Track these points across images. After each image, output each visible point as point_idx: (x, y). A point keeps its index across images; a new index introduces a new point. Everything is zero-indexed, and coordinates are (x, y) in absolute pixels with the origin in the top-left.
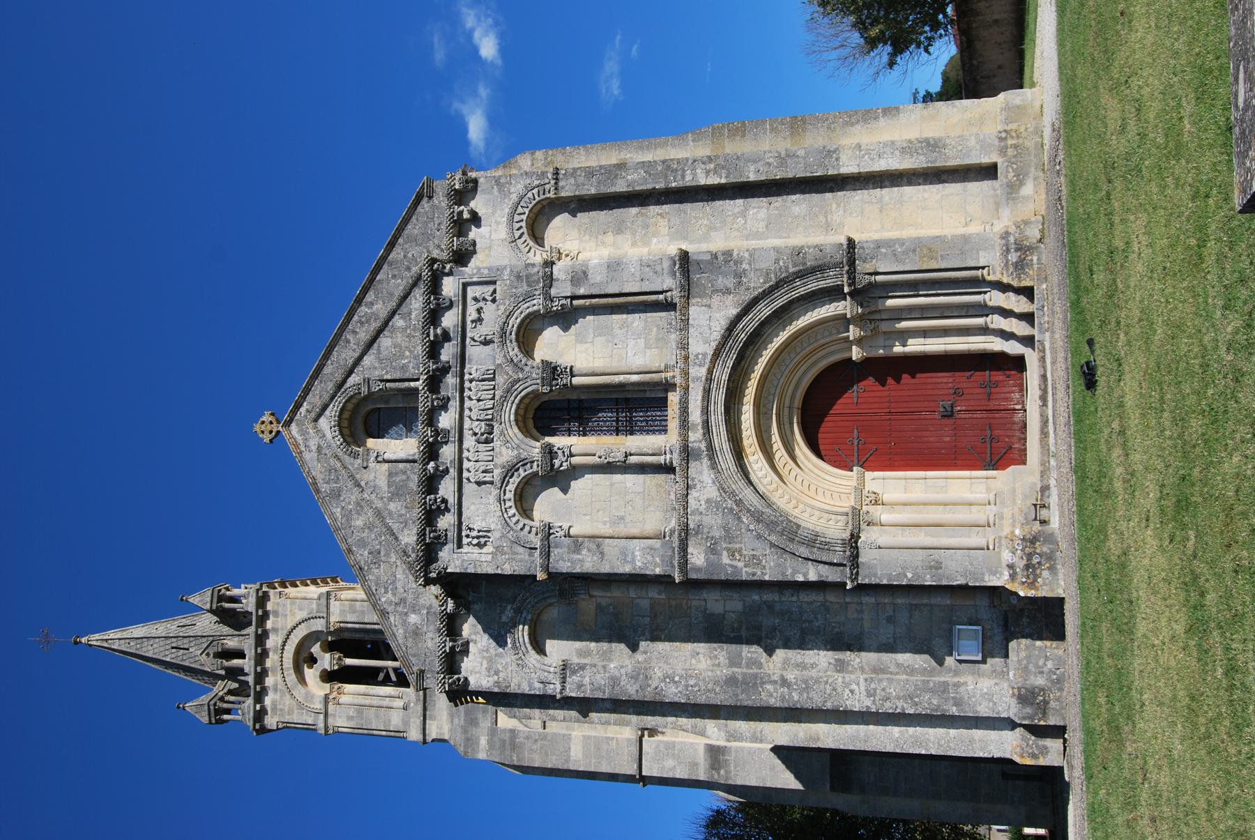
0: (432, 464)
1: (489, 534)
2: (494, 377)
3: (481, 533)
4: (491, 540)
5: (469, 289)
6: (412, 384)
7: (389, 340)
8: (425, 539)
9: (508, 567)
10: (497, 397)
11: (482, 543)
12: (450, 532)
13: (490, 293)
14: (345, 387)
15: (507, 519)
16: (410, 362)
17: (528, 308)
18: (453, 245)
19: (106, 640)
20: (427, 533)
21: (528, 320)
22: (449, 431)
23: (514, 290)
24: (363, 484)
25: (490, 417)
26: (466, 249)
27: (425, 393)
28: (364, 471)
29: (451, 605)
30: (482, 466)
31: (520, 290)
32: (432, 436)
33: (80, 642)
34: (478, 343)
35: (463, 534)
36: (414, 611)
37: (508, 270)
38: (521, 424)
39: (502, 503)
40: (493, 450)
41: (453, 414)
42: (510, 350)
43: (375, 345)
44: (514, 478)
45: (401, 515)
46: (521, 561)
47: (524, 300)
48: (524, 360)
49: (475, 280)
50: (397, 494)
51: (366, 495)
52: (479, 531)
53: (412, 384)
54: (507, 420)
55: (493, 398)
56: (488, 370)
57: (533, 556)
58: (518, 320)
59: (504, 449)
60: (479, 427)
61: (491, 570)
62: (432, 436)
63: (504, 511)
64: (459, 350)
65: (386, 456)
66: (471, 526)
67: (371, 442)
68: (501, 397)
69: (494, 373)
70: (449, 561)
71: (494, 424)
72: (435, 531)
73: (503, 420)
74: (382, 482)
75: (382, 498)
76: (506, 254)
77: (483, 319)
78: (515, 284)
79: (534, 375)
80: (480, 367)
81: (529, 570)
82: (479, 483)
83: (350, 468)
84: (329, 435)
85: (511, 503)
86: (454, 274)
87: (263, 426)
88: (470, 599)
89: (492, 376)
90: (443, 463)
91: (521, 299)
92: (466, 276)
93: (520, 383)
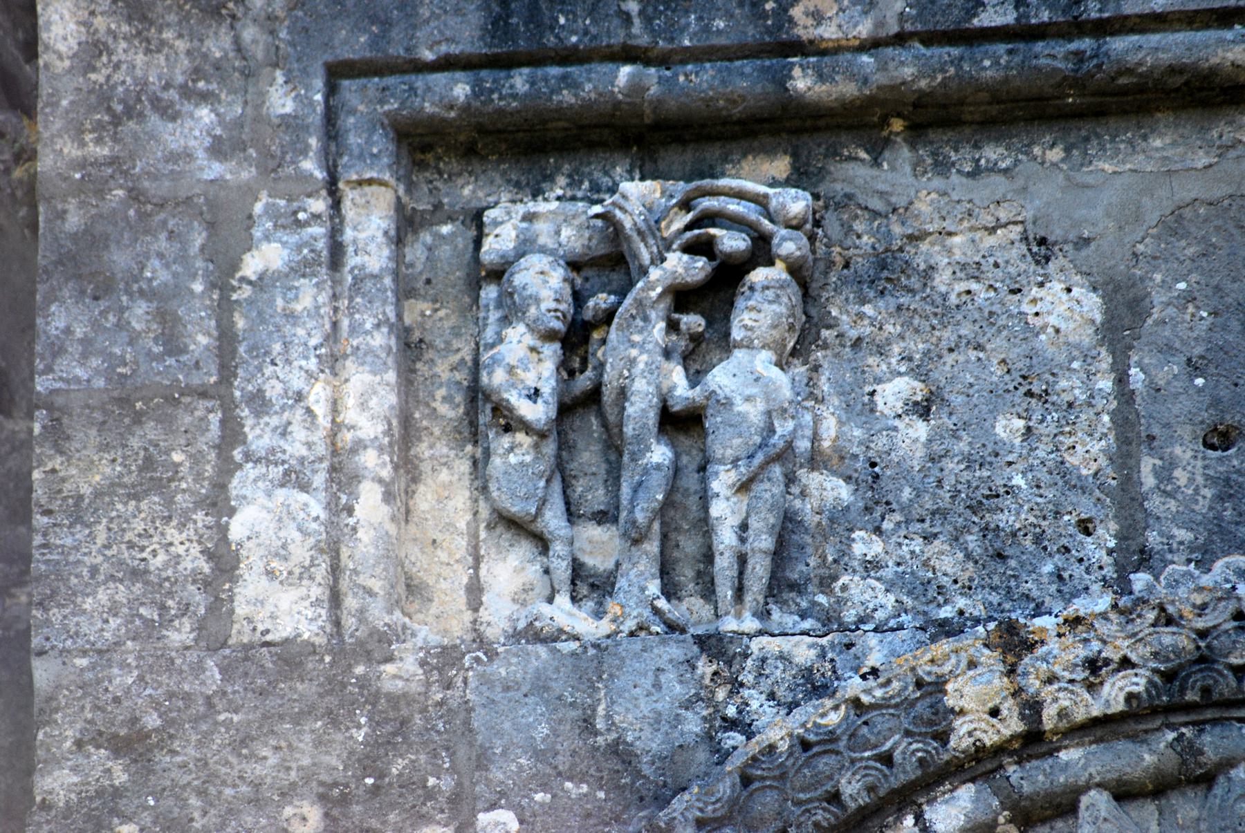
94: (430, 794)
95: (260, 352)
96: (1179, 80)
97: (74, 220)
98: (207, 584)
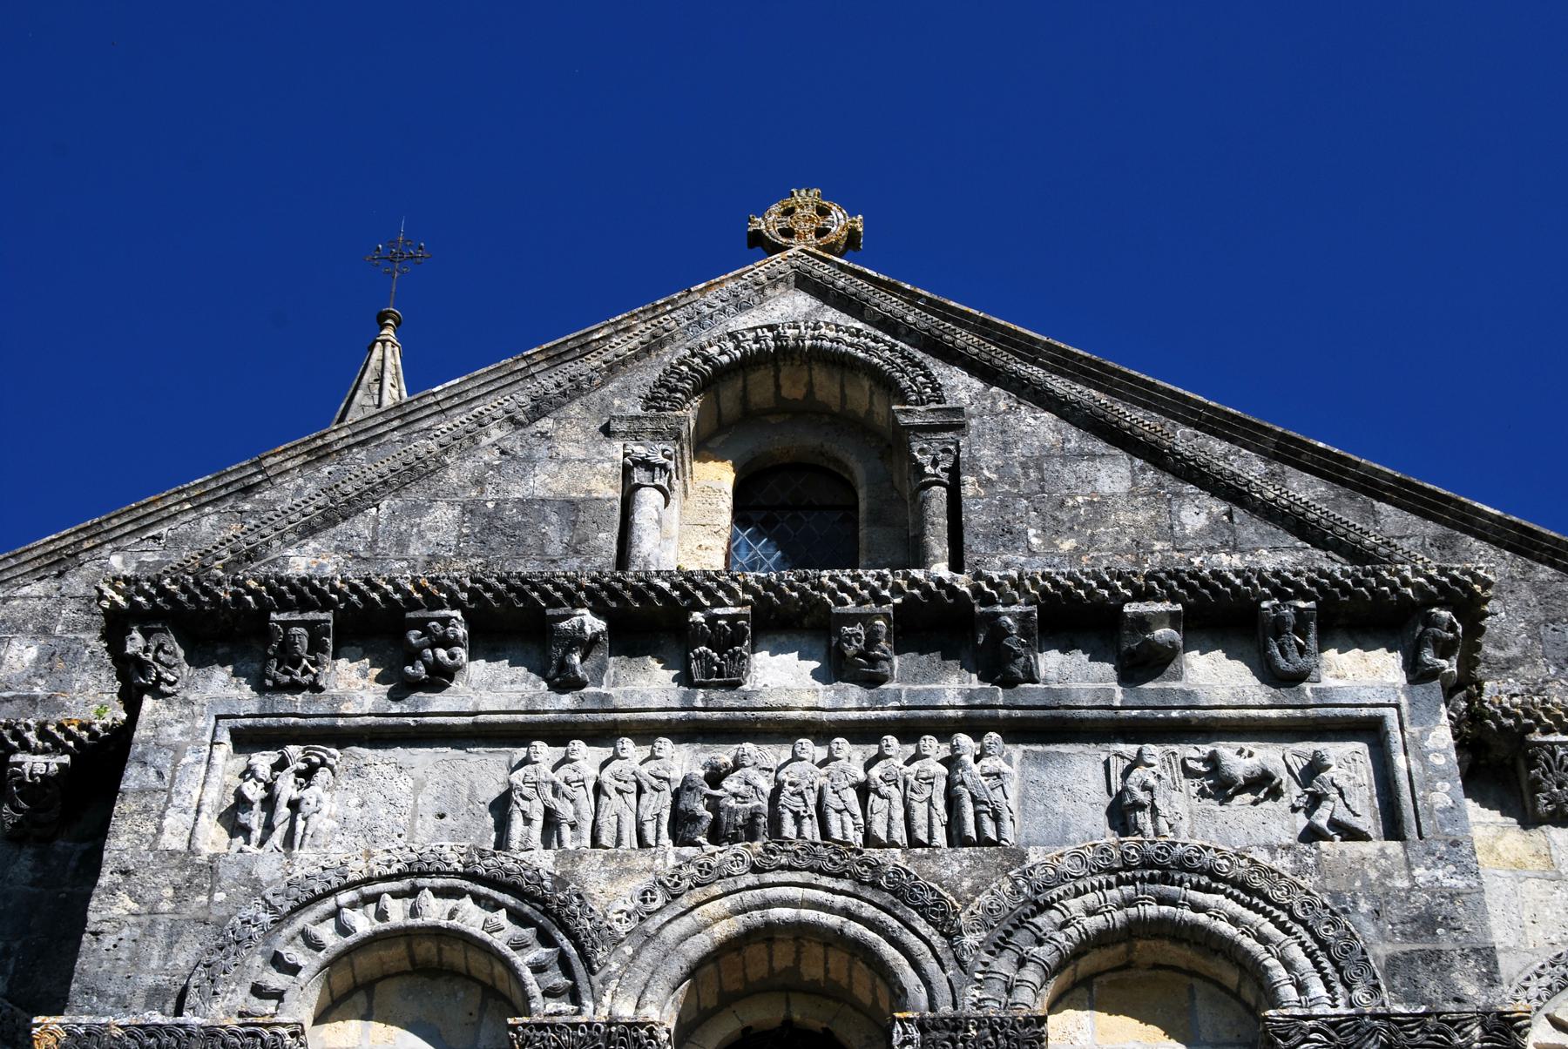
0: (593, 624)
1: (277, 838)
2: (966, 842)
3: (283, 811)
4: (252, 848)
5: (1358, 749)
6: (939, 547)
7: (1122, 486)
8: (285, 606)
9: (117, 911)
10: (875, 854)
11: (243, 818)
12: (307, 702)
13: (1343, 815)
14: (929, 361)
15: (330, 904)
16: (1032, 553)
17: (1289, 965)
18: (1547, 730)
19: (380, 380)
20: (311, 616)
21: (1231, 977)
22: (734, 686)
23: (1365, 906)
24: (546, 424)
25: (789, 829)
26: (1536, 786)
27: (897, 589)
28: (595, 427)
29: (36, 764)
30: (577, 808)
31: (1369, 930)
32: (712, 620)
33: (383, 327)
34: (1117, 785)
35: (294, 751)
36: (48, 656)
37: (1459, 883)
38: (757, 962)
39: (405, 884)
41: (807, 699)
42: (1091, 899)
43: (1100, 446)
44: (512, 930)
45: (402, 543)
46: (136, 960)
47: (1323, 945)
48: (1044, 952)
49: (1400, 761)
50: (490, 528)
51: (496, 434)
52: (294, 805)
53: (939, 547)
54: (771, 893)
55: (870, 839)
56: (997, 818)
57: (149, 1005)
58: (1224, 927)
59: (641, 882)
60: (742, 789)
61: (120, 844)
62: (712, 620)
63: (367, 890)
64: (1084, 713)
65: (649, 499)
66: (323, 775)
67: (718, 477)
68: (875, 868)
69: (983, 841)
70: (187, 702)
71: (757, 846)
72: (316, 646)
73: (769, 877)
74: (542, 482)
75: (479, 482)
76: (1536, 935)
77: (1225, 799)
78: (1395, 912)
79: (972, 993)
80: (1013, 794)
81: (88, 990)
82: (502, 808)
83: (611, 387)
84: (741, 322)
85: (398, 913)
86: (1419, 689)
87: (810, 211)
88: (60, 845)
89: (971, 830)
90: (601, 669)
91: (1330, 934)
92: (1413, 730)
93: (936, 940)
94: (203, 888)
95: (181, 781)
96: (441, 730)
97: (140, 749)
98: (154, 835)
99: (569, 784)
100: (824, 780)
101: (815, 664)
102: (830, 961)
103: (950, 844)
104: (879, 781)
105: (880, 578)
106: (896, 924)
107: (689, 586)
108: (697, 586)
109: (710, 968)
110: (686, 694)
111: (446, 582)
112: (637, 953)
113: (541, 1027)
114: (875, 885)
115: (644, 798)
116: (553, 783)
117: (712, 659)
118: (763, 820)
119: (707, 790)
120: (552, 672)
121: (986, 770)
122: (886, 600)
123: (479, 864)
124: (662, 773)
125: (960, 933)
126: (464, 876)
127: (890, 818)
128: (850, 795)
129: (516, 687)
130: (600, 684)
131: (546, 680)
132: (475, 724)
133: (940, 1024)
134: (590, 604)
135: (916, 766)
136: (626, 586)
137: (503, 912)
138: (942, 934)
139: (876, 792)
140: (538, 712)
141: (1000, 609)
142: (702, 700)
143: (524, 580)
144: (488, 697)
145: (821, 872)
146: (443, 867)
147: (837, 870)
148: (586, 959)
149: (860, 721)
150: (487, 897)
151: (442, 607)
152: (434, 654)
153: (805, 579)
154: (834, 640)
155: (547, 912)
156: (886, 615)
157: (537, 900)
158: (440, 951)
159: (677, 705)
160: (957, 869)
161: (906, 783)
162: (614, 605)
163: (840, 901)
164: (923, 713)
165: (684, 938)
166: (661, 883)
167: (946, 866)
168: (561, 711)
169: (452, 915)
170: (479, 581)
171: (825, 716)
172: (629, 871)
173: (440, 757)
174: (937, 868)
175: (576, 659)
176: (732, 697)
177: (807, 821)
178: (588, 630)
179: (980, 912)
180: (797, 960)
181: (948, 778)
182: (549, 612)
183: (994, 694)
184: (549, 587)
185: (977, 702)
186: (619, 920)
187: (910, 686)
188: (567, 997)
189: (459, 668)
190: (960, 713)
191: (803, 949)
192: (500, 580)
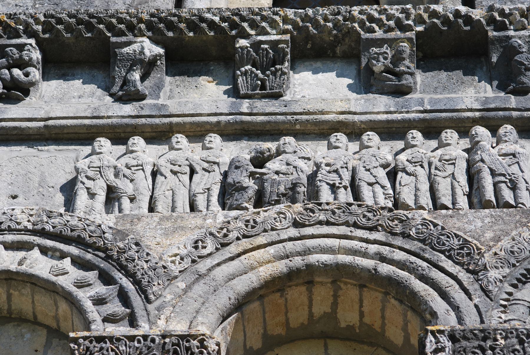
2: (487, 205)
22: (277, 96)
25: (326, 195)
27: (419, 20)
32: (256, 45)
40: (193, 207)
44: (75, 273)
54: (310, 243)
56: (514, 188)
71: (298, 207)
89: (490, 194)
90: (159, 87)
93: (463, 276)
96: (15, 132)
99: (130, 168)
100: (356, 163)
101: (351, 81)
102: (365, 303)
103: (471, 206)
104: (407, 163)
105: (403, 11)
106: (425, 264)
107: (236, 18)
108: (243, 19)
109: (255, 305)
110: (233, 103)
111: (22, 17)
112: (189, 288)
113: (100, 339)
114: (406, 236)
115: (195, 177)
116: (115, 167)
117: (256, 75)
118: (302, 189)
119: (252, 169)
120: (115, 89)
121: (503, 152)
122: (409, 28)
123: (47, 222)
124: (211, 159)
125: (485, 269)
126: (34, 232)
127: (417, 189)
128: (380, 172)
129: (82, 100)
130: (158, 97)
131: (111, 95)
132: (46, 126)
133: (470, 335)
134: (150, 34)
135: (439, 152)
136: (181, 19)
137: (68, 260)
138: (468, 271)
139: (404, 170)
140: (102, 117)
141: (511, 33)
142: (248, 108)
143: (91, 16)
144: (58, 107)
145: (356, 225)
146: (13, 226)
147: (370, 224)
148: (143, 291)
149: (388, 122)
150: (54, 250)
151: (19, 37)
152: (11, 73)
153: (339, 13)
154: (364, 62)
155: (108, 258)
156: (410, 40)
157: (99, 249)
158: (9, 297)
159: (226, 111)
160: (479, 224)
161: (430, 164)
162: (171, 34)
163: (373, 248)
164: (444, 115)
165: (232, 277)
166: (211, 234)
167: (470, 222)
168: (123, 117)
169: (20, 263)
170: (52, 16)
171: (356, 118)
172: (182, 228)
173: (14, 154)
174: (461, 224)
175: (136, 76)
176: (273, 105)
177: (342, 190)
178: (148, 53)
179: (503, 253)
180: (335, 305)
181: (468, 161)
182: (114, 39)
183: (508, 100)
184: (114, 21)
185: (492, 106)
186: (173, 262)
187: (432, 96)
188: (126, 322)
189: (33, 84)
190: (477, 114)
191: (340, 293)
192: (70, 16)
